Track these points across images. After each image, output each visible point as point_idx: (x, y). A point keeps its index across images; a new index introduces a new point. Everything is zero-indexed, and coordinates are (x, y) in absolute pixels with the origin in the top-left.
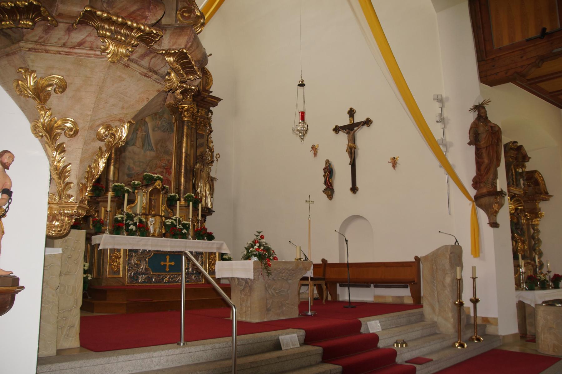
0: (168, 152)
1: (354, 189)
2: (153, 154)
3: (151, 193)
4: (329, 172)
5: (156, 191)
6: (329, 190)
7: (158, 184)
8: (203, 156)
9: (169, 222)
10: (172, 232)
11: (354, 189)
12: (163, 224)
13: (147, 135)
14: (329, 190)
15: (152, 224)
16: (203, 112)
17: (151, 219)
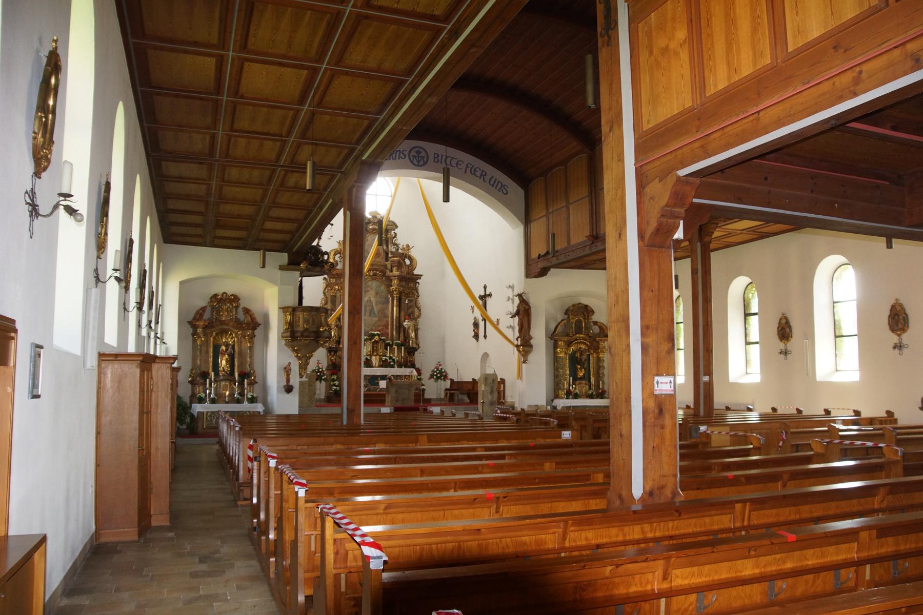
0: (386, 316)
1: (485, 337)
2: (376, 319)
3: (373, 343)
4: (476, 325)
5: (376, 342)
6: (476, 336)
7: (376, 338)
8: (413, 313)
9: (384, 358)
10: (384, 364)
11: (485, 337)
12: (381, 359)
13: (372, 306)
14: (476, 336)
15: (375, 360)
16: (411, 285)
17: (374, 358)
